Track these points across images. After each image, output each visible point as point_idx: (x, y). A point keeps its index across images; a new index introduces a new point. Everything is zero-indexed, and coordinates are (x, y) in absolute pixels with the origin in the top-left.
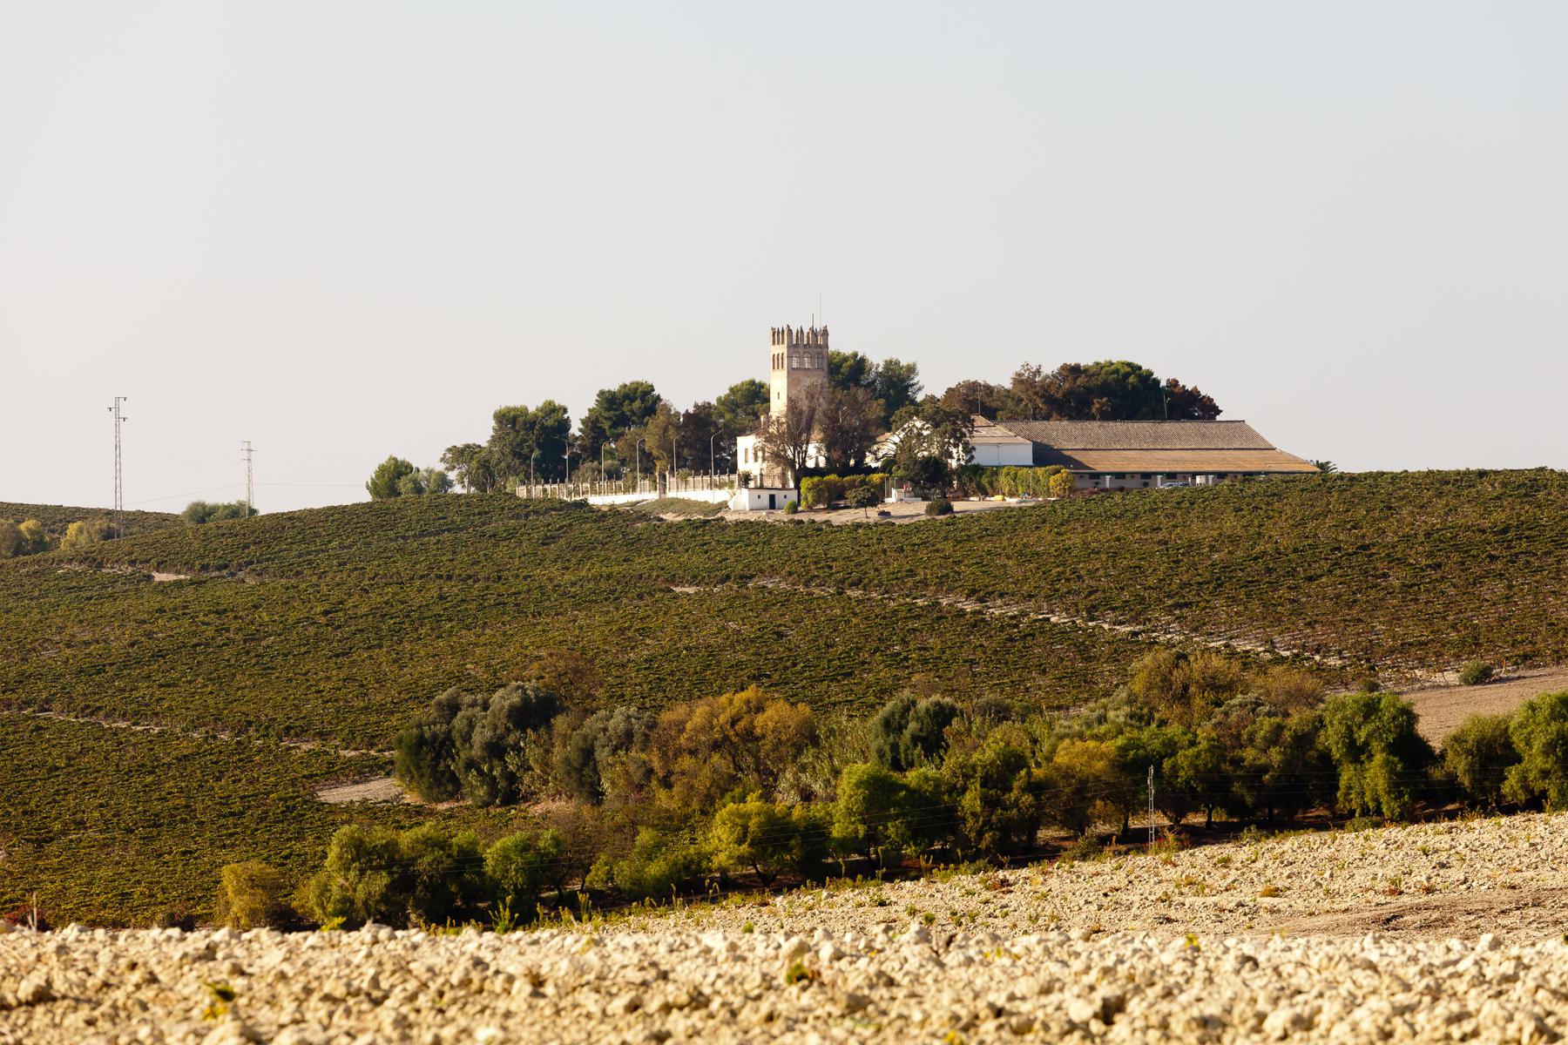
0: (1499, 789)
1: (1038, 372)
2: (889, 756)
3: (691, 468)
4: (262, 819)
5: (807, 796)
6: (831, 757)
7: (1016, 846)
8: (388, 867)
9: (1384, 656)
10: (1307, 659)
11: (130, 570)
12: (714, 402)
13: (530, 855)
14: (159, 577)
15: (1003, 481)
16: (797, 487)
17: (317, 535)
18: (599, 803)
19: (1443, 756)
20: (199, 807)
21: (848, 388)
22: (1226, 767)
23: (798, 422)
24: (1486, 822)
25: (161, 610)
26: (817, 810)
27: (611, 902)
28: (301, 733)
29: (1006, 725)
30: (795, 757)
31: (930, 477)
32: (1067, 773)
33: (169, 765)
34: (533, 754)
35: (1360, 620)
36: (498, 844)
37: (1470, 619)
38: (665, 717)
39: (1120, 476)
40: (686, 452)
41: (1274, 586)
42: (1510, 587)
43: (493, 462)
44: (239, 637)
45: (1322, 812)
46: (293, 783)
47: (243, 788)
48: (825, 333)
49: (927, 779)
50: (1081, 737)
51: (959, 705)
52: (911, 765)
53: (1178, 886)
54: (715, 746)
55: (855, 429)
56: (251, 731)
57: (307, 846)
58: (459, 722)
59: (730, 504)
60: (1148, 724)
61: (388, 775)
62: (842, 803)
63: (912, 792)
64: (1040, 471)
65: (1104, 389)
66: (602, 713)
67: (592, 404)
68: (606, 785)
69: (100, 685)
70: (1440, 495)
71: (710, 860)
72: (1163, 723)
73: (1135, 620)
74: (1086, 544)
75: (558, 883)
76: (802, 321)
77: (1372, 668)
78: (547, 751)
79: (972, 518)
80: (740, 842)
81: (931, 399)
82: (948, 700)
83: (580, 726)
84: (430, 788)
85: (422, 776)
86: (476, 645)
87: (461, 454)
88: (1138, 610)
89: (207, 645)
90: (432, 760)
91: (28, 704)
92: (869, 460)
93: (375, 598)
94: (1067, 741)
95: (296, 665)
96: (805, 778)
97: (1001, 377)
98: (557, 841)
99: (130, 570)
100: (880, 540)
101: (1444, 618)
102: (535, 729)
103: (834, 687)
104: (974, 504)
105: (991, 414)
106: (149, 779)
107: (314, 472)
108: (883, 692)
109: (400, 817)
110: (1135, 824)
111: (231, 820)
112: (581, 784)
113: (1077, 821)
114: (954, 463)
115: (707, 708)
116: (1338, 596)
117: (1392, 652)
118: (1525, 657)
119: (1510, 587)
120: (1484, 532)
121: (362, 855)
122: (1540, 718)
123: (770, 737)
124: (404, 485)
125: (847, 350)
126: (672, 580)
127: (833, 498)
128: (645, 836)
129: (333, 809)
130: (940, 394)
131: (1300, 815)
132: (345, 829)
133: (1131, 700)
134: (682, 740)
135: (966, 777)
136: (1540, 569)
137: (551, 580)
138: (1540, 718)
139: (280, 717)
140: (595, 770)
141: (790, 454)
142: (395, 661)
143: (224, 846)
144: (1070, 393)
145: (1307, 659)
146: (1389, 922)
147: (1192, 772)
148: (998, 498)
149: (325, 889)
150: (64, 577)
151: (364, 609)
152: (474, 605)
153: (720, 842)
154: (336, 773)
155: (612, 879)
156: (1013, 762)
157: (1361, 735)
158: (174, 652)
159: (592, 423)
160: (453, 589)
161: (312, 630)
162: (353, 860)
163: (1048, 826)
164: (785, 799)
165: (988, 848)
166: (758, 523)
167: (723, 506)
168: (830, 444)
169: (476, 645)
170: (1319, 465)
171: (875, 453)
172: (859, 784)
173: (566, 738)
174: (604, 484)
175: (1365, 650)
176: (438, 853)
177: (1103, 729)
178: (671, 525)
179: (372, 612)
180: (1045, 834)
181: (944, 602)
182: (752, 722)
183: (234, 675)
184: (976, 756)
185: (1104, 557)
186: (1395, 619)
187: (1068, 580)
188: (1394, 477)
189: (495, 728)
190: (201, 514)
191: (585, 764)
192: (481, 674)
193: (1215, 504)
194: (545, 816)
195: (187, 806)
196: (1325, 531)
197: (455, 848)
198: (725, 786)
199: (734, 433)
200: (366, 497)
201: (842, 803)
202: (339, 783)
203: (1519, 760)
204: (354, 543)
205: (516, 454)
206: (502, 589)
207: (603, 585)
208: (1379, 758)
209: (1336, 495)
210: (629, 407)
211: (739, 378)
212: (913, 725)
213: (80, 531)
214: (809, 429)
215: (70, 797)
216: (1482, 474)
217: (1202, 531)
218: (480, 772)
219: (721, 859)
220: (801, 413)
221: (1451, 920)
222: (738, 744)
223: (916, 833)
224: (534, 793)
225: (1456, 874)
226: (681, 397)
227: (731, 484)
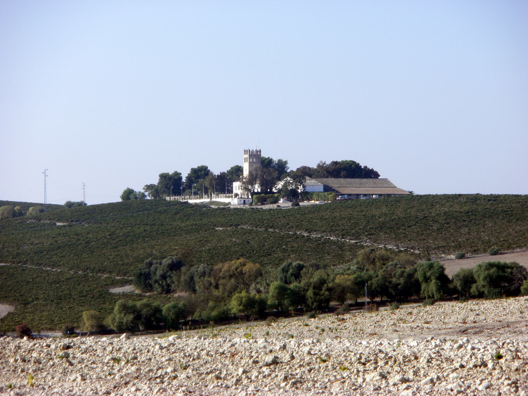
0: (469, 291)
1: (325, 163)
2: (284, 279)
3: (219, 192)
4: (93, 298)
5: (259, 292)
6: (266, 280)
7: (322, 307)
8: (133, 312)
9: (432, 250)
10: (409, 251)
11: (49, 222)
12: (226, 172)
13: (176, 309)
14: (58, 224)
15: (315, 196)
16: (252, 198)
17: (106, 211)
18: (195, 293)
19: (452, 280)
20: (73, 294)
21: (267, 168)
22: (387, 284)
23: (252, 178)
24: (487, 301)
25: (59, 234)
26: (263, 296)
27: (197, 324)
28: (104, 271)
29: (319, 271)
30: (255, 280)
31: (292, 195)
32: (339, 285)
33: (64, 281)
34: (175, 278)
35: (425, 239)
36: (167, 306)
37: (458, 239)
38: (216, 267)
39: (349, 195)
40: (217, 187)
41: (398, 228)
42: (470, 230)
43: (159, 189)
44: (84, 242)
45: (416, 297)
46: (102, 286)
47: (86, 288)
48: (260, 151)
49: (296, 287)
50: (343, 274)
51: (305, 264)
52: (291, 283)
53: (398, 321)
54: (231, 277)
55: (269, 180)
56: (88, 271)
57: (107, 306)
58: (152, 268)
59: (232, 203)
60: (363, 270)
61: (130, 284)
62: (271, 294)
63: (292, 291)
64: (326, 193)
65: (345, 169)
66: (196, 266)
67: (189, 172)
68: (197, 288)
69: (41, 257)
70: (448, 201)
71: (231, 311)
72: (367, 270)
73: (356, 239)
74: (341, 216)
75: (184, 317)
76: (253, 148)
77: (429, 254)
78: (179, 278)
79: (305, 207)
80: (240, 305)
81: (292, 171)
82: (301, 263)
83: (190, 270)
84: (143, 288)
85: (141, 285)
86: (156, 245)
87: (149, 187)
88: (357, 236)
89: (74, 245)
90: (144, 280)
91: (20, 262)
92: (274, 190)
93: (125, 231)
94: (339, 276)
95: (101, 251)
96: (258, 286)
97: (313, 165)
98: (184, 305)
99: (49, 222)
100: (278, 214)
101: (450, 239)
102: (176, 271)
103: (265, 259)
104: (305, 203)
105: (310, 176)
106: (58, 285)
107: (105, 192)
108: (280, 260)
109: (135, 297)
110: (359, 300)
111: (83, 298)
112: (189, 287)
113: (341, 299)
114: (299, 191)
115: (228, 265)
116: (418, 232)
117: (435, 249)
118: (475, 251)
119: (470, 230)
120: (461, 213)
121: (125, 308)
122: (482, 269)
123: (247, 274)
124: (131, 196)
125: (266, 157)
126: (215, 226)
127: (263, 201)
128: (211, 304)
129: (114, 295)
130: (295, 170)
131: (409, 298)
132: (120, 301)
133: (358, 263)
134: (221, 274)
135: (308, 286)
136: (479, 224)
137: (178, 225)
138: (482, 269)
139: (97, 267)
140: (194, 283)
141: (250, 188)
142: (131, 250)
143: (81, 306)
144: (334, 170)
145: (409, 251)
146: (464, 332)
147: (377, 285)
148: (313, 201)
149: (114, 319)
150: (29, 224)
151: (121, 234)
152: (155, 233)
153: (234, 306)
154: (115, 284)
155: (201, 316)
156: (322, 282)
157: (428, 274)
158: (64, 247)
159: (189, 178)
160: (148, 228)
161: (105, 240)
162: (123, 310)
163: (333, 301)
164: (253, 293)
165: (315, 308)
166: (240, 209)
167: (229, 203)
168: (262, 185)
169: (156, 245)
170: (409, 192)
171: (275, 188)
172: (276, 288)
173: (185, 274)
174: (193, 196)
175: (426, 248)
176: (148, 309)
177: (349, 272)
178: (214, 209)
179: (124, 235)
180: (332, 303)
181: (298, 233)
182: (242, 269)
183: (82, 254)
184: (311, 280)
185: (346, 220)
186: (435, 239)
187: (336, 226)
188: (434, 196)
189: (164, 270)
190: (70, 205)
191: (191, 281)
192: (158, 254)
193: (380, 204)
194: (180, 297)
195: (70, 294)
196: (413, 212)
197: (153, 307)
198: (235, 289)
199: (231, 181)
200: (120, 200)
201: (271, 294)
202: (115, 287)
203: (476, 282)
204: (117, 214)
205: (166, 187)
206: (163, 228)
207: (194, 227)
208: (434, 281)
209: (416, 201)
210: (200, 174)
211: (233, 165)
212: (291, 271)
213: (33, 210)
214: (255, 180)
215: (34, 290)
216: (460, 195)
217: (377, 213)
218: (159, 284)
219: (234, 310)
220: (253, 175)
221: (483, 331)
222: (238, 275)
223: (294, 303)
224: (175, 290)
225: (482, 317)
226: (216, 170)
227: (232, 197)
